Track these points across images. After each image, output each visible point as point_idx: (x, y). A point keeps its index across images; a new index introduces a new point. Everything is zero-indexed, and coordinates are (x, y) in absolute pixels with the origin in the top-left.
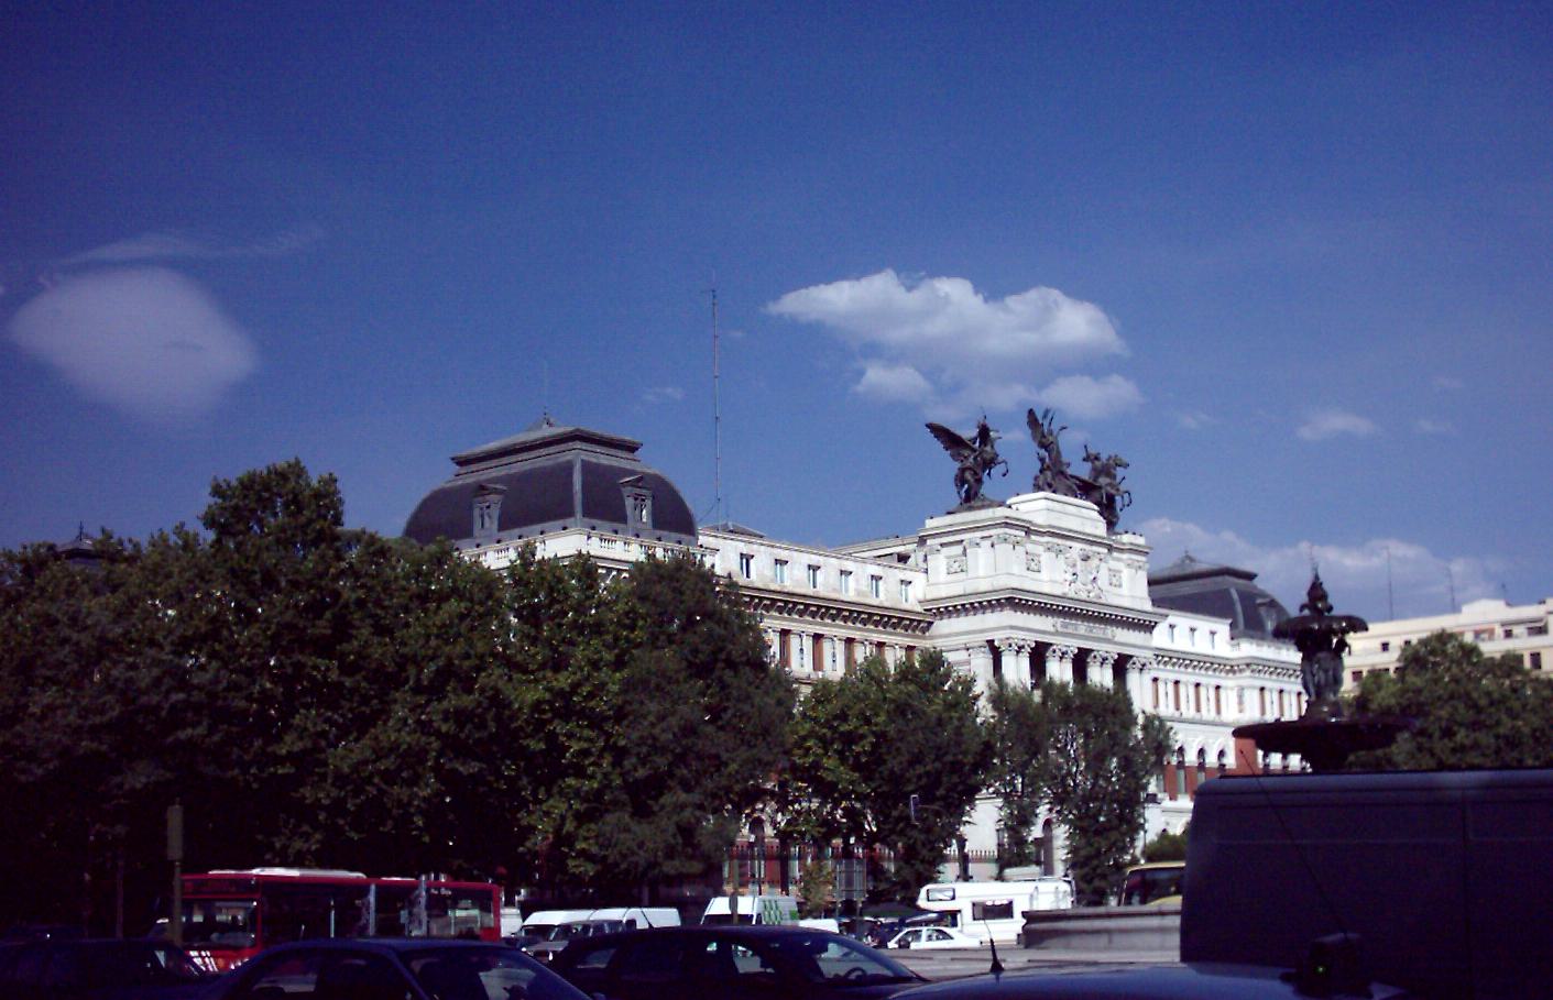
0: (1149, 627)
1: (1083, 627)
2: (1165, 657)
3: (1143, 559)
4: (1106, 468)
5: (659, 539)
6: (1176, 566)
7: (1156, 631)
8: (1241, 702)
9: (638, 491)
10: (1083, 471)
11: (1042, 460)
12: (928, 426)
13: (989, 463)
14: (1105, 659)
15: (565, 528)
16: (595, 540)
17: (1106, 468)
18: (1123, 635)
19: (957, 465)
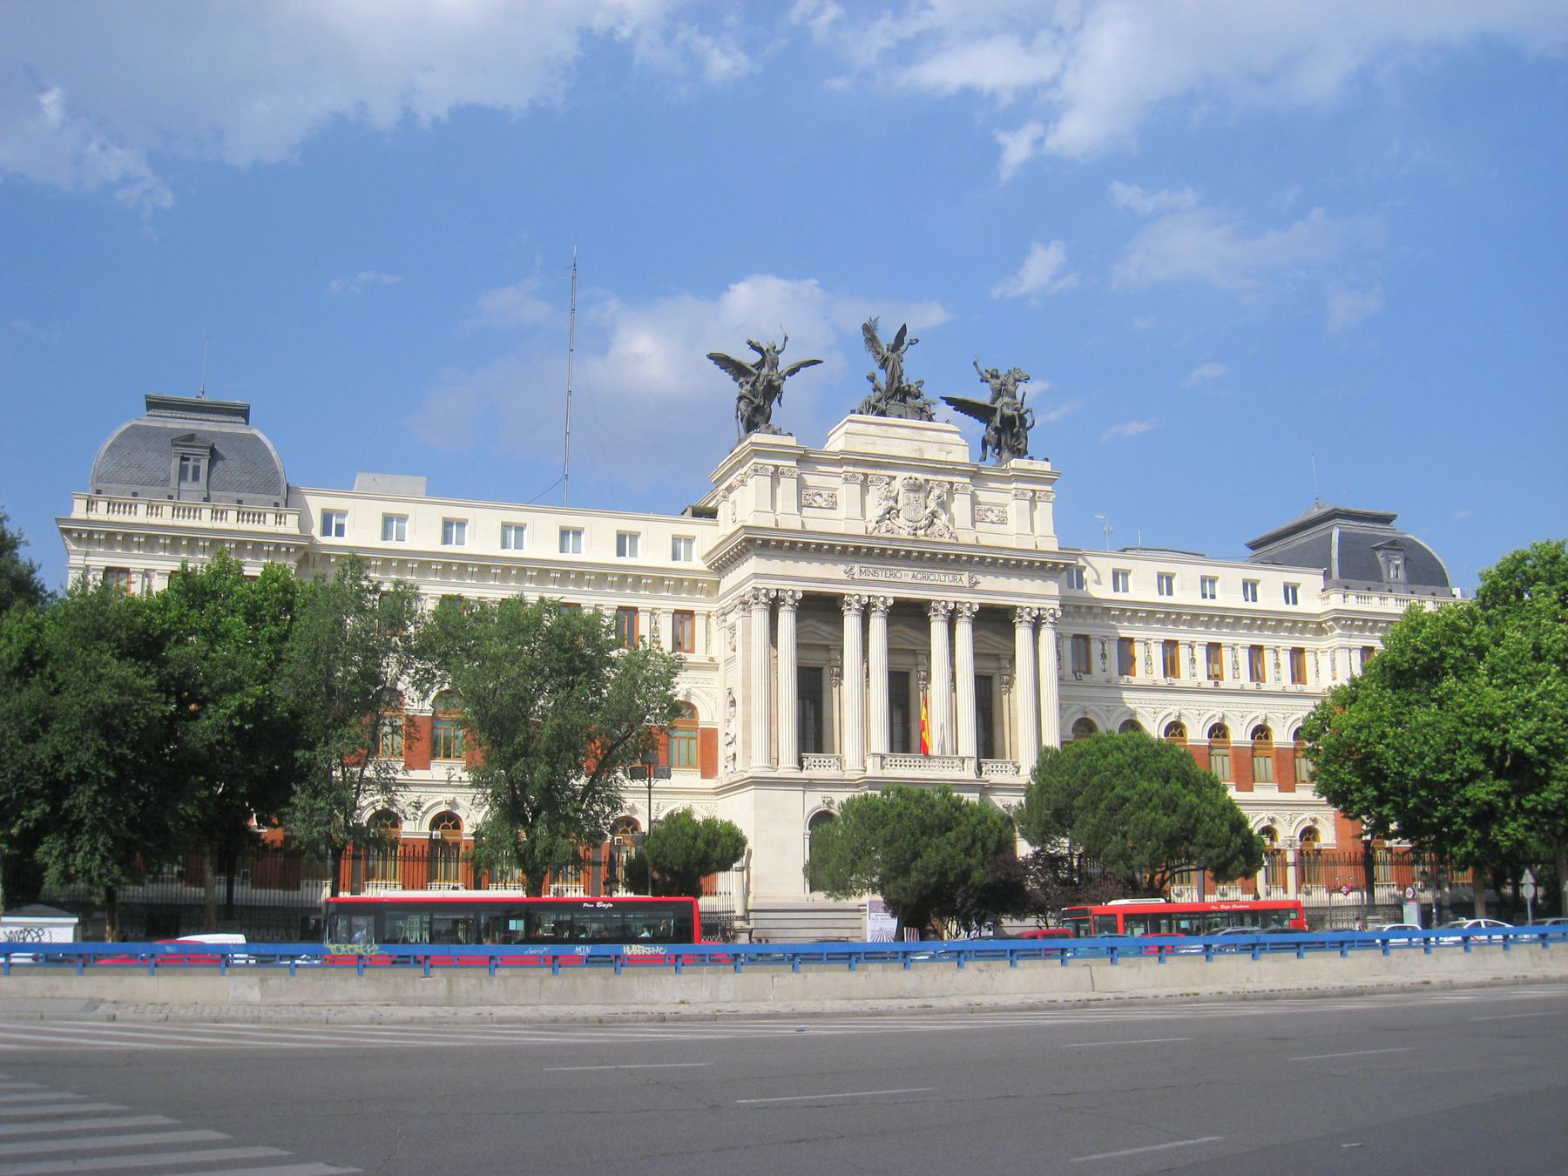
3: (1049, 488)
10: (983, 396)
11: (872, 379)
12: (711, 357)
16: (1352, 599)
18: (989, 582)
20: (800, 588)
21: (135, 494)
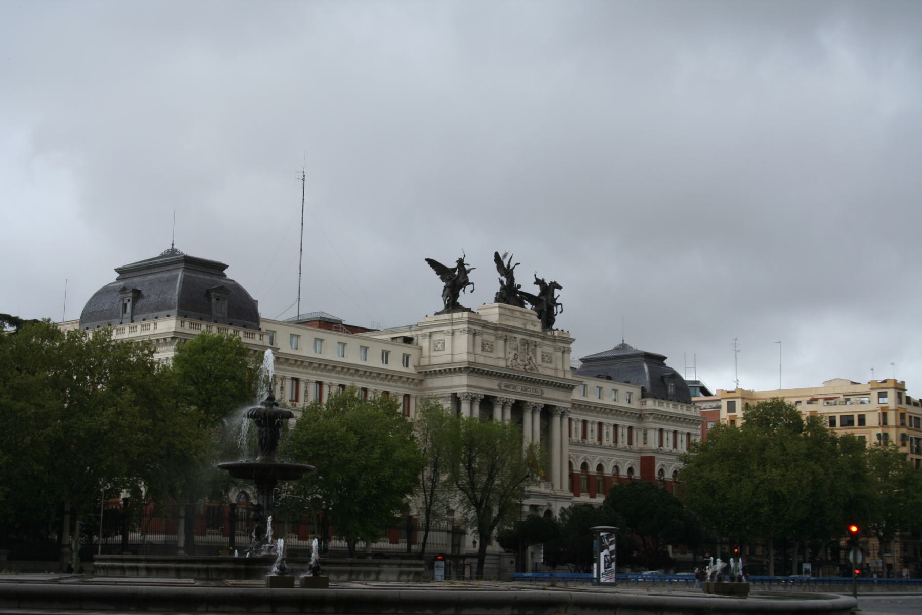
0: (569, 388)
1: (520, 387)
2: (579, 406)
4: (548, 289)
5: (231, 324)
6: (616, 349)
7: (574, 391)
8: (645, 438)
9: (219, 295)
10: (536, 291)
11: (501, 282)
12: (427, 260)
13: (466, 283)
14: (535, 408)
15: (168, 316)
17: (548, 289)
19: (444, 284)
20: (482, 393)
21: (201, 319)
